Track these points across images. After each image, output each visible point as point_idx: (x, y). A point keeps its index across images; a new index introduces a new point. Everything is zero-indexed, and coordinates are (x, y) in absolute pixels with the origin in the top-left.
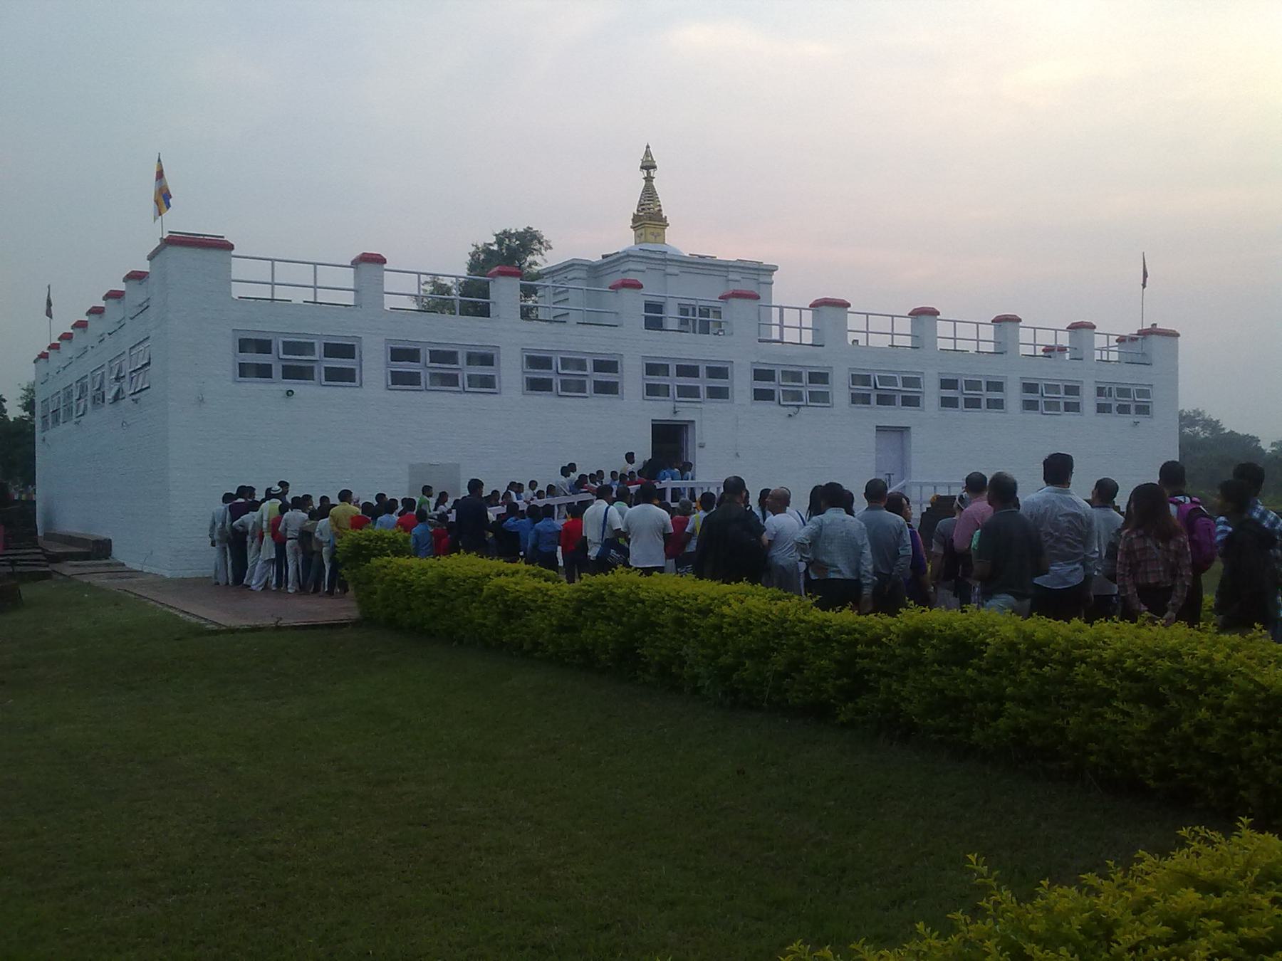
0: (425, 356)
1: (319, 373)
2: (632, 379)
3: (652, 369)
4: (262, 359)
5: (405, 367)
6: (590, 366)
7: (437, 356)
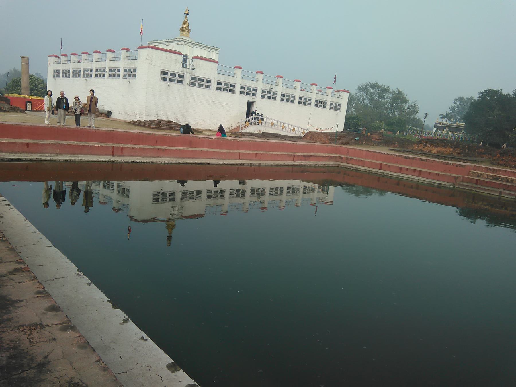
0: (197, 79)
1: (176, 81)
2: (237, 89)
4: (165, 76)
6: (229, 85)
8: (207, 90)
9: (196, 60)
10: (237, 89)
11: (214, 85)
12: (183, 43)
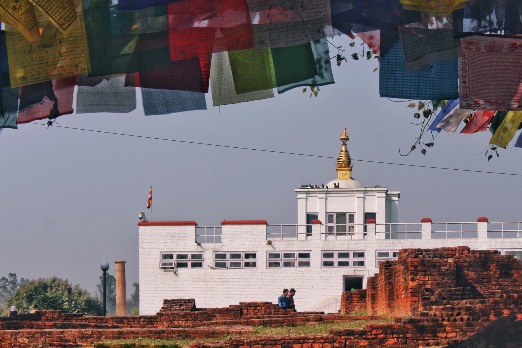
0: (228, 256)
2: (316, 259)
3: (326, 255)
5: (221, 260)
7: (234, 256)
8: (249, 269)
9: (225, 228)
10: (316, 259)
11: (262, 260)
12: (304, 196)
